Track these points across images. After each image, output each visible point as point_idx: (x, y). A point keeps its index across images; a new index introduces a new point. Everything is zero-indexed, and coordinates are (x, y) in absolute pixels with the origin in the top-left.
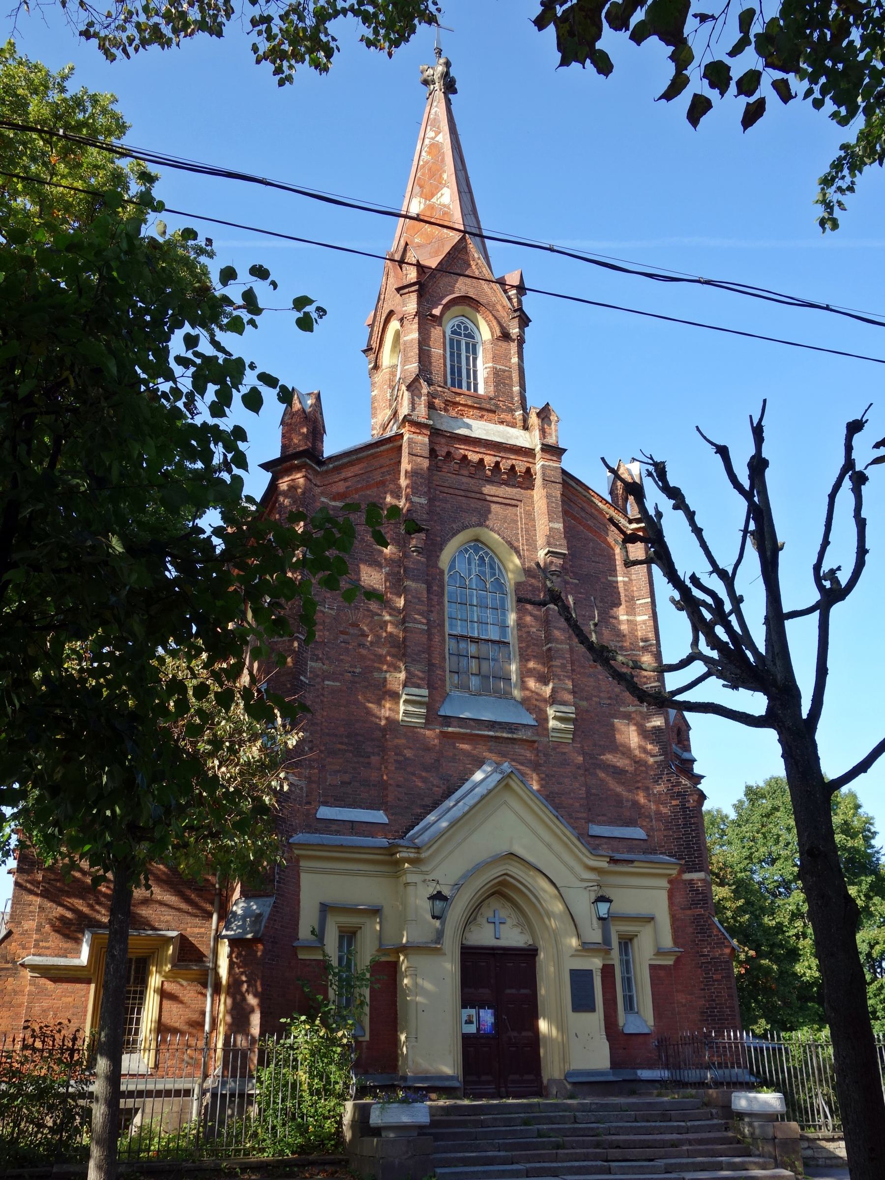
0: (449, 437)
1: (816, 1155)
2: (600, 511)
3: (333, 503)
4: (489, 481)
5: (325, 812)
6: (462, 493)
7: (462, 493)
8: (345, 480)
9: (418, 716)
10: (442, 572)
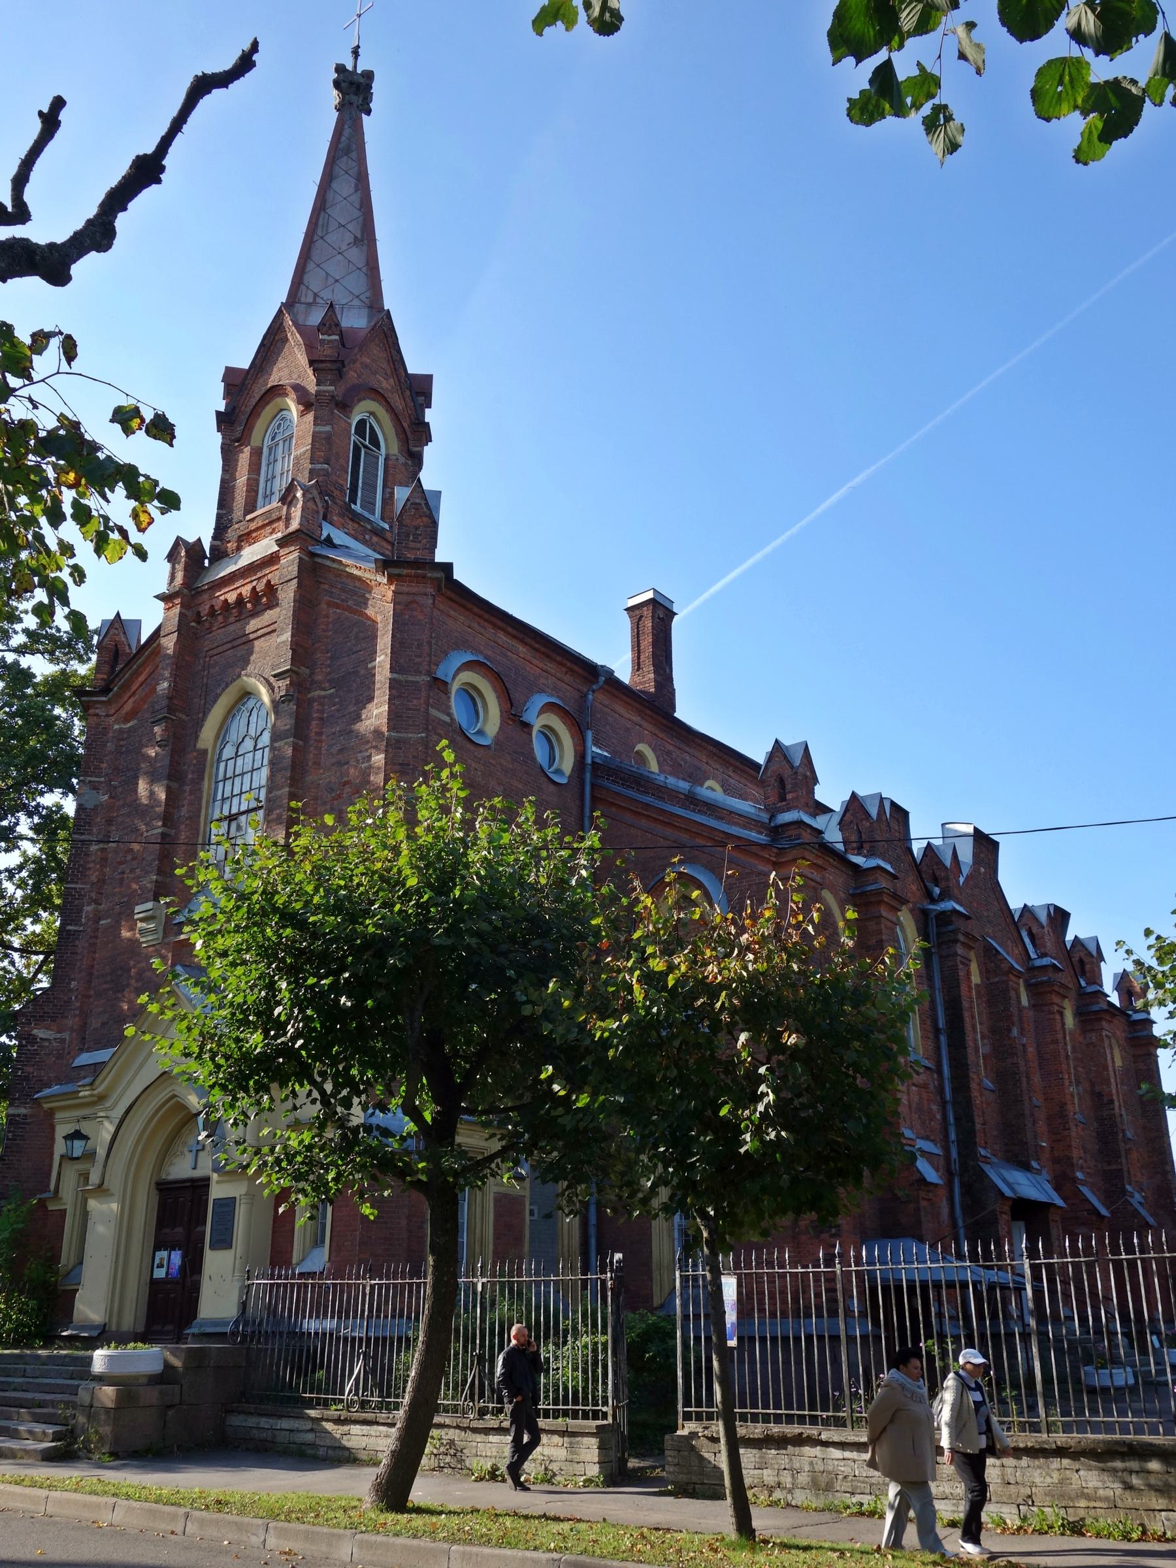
0: (209, 589)
1: (318, 1442)
2: (359, 579)
3: (129, 725)
4: (254, 614)
5: (84, 1059)
6: (229, 645)
7: (229, 645)
8: (134, 693)
9: (154, 931)
10: (205, 751)
